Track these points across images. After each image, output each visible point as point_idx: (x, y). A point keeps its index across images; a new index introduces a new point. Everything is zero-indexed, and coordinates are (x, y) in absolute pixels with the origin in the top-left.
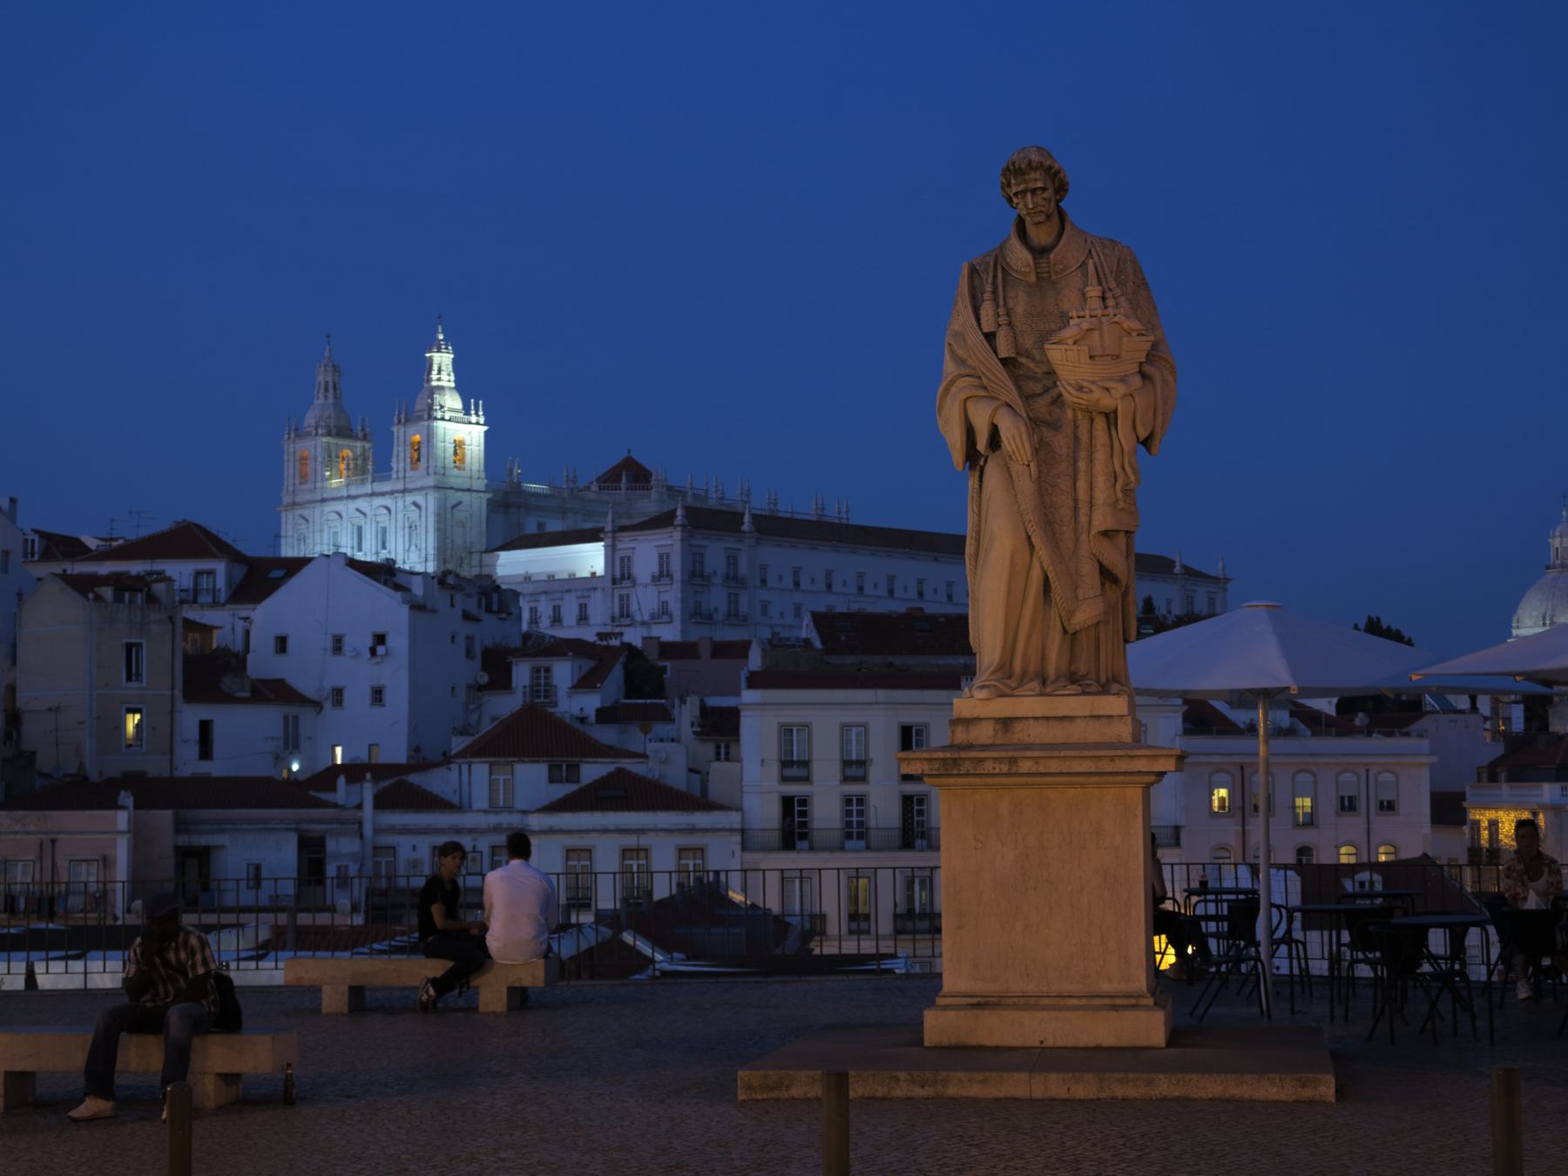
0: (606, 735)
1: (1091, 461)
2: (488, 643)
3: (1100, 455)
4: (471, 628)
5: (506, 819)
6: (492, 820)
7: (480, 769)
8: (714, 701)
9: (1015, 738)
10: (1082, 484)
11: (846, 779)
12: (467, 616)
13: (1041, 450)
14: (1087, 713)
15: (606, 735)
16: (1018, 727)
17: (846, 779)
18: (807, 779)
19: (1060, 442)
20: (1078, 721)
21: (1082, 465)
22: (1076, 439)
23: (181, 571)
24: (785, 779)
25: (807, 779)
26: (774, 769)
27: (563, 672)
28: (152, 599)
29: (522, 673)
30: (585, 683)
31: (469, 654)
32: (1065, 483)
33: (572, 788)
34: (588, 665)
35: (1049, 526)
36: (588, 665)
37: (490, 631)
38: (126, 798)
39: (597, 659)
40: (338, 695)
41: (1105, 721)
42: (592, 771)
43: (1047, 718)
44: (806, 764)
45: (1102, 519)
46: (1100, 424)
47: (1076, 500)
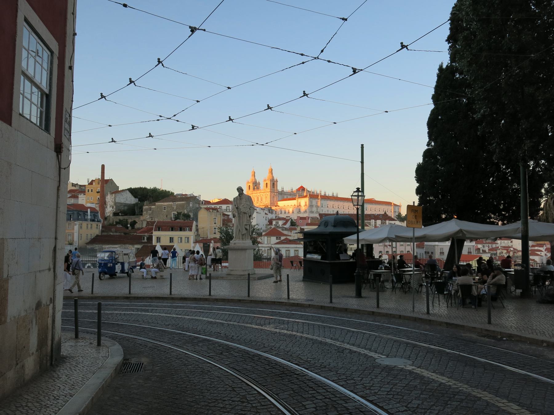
0: (285, 232)
2: (270, 218)
4: (266, 216)
5: (269, 245)
6: (267, 245)
7: (266, 238)
8: (302, 227)
12: (266, 214)
13: (239, 217)
15: (285, 232)
19: (241, 216)
23: (224, 207)
27: (281, 223)
28: (218, 211)
29: (274, 223)
30: (285, 224)
33: (278, 241)
34: (284, 221)
35: (240, 224)
36: (284, 221)
37: (270, 216)
38: (212, 242)
39: (286, 220)
42: (283, 238)
45: (245, 223)
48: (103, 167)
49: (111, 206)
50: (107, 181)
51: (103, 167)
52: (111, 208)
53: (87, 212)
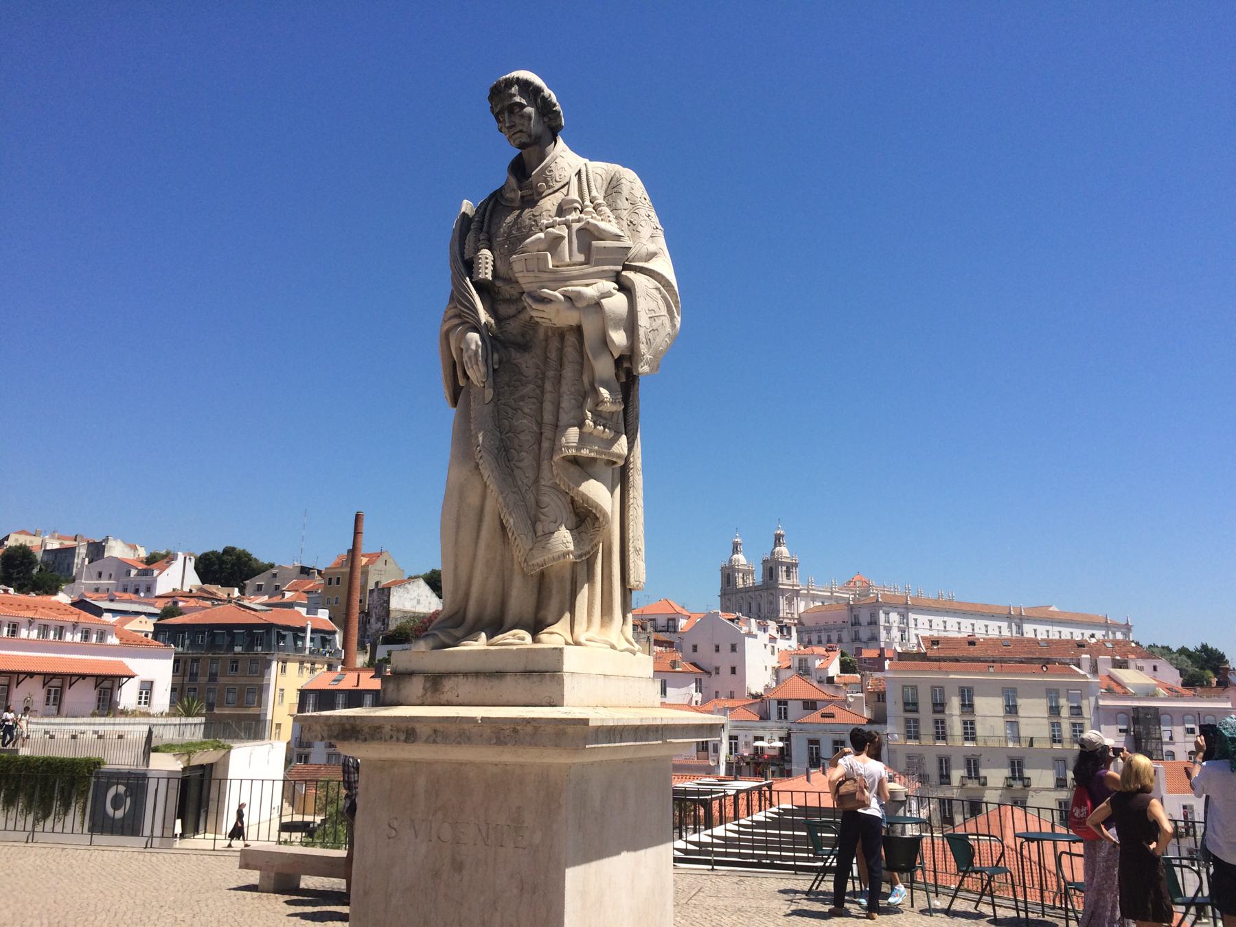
1: (559, 380)
3: (569, 372)
9: (444, 698)
10: (548, 407)
11: (935, 712)
14: (521, 667)
16: (448, 684)
17: (935, 712)
18: (916, 711)
20: (508, 678)
21: (548, 386)
22: (546, 360)
24: (906, 711)
25: (916, 711)
26: (901, 706)
31: (773, 653)
32: (528, 407)
40: (717, 670)
41: (535, 678)
43: (477, 674)
44: (915, 704)
46: (571, 339)
47: (540, 424)
48: (358, 518)
49: (378, 620)
50: (374, 557)
51: (358, 518)
52: (379, 624)
53: (303, 630)
